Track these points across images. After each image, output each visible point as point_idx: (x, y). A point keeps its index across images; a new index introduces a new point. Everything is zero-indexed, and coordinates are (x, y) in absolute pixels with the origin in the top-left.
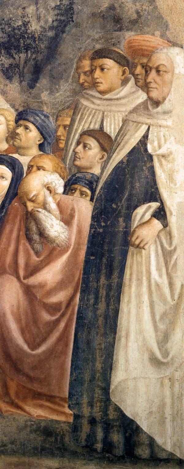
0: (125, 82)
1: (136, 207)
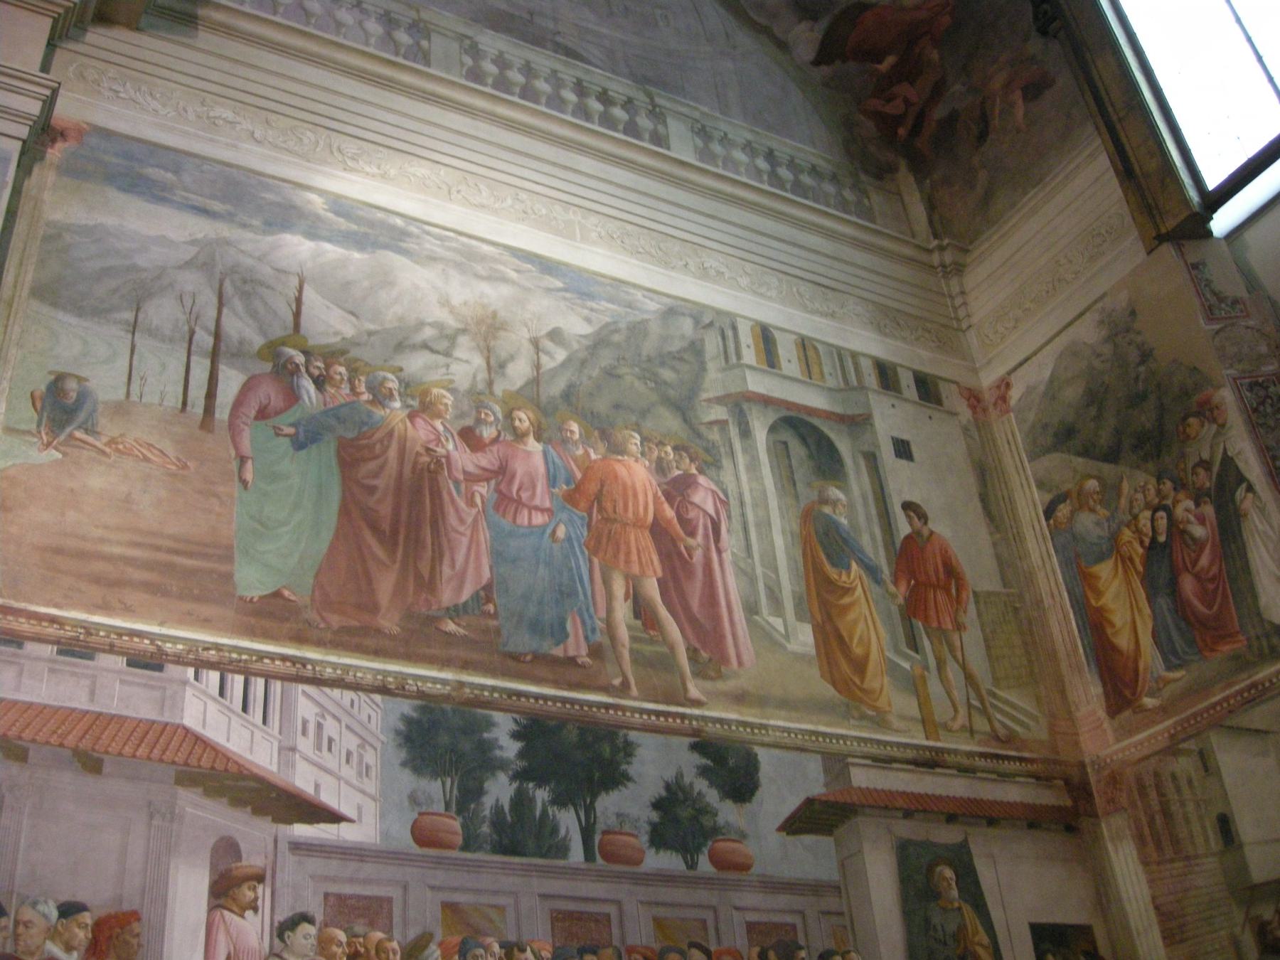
0: (1203, 426)
1: (1235, 491)
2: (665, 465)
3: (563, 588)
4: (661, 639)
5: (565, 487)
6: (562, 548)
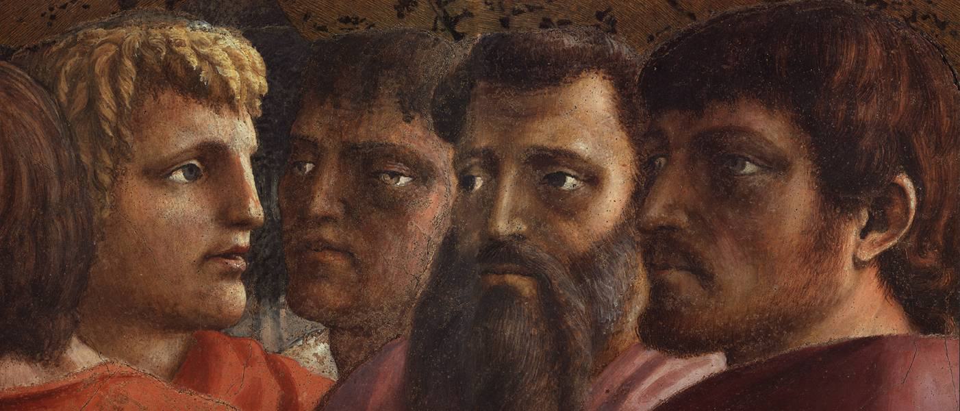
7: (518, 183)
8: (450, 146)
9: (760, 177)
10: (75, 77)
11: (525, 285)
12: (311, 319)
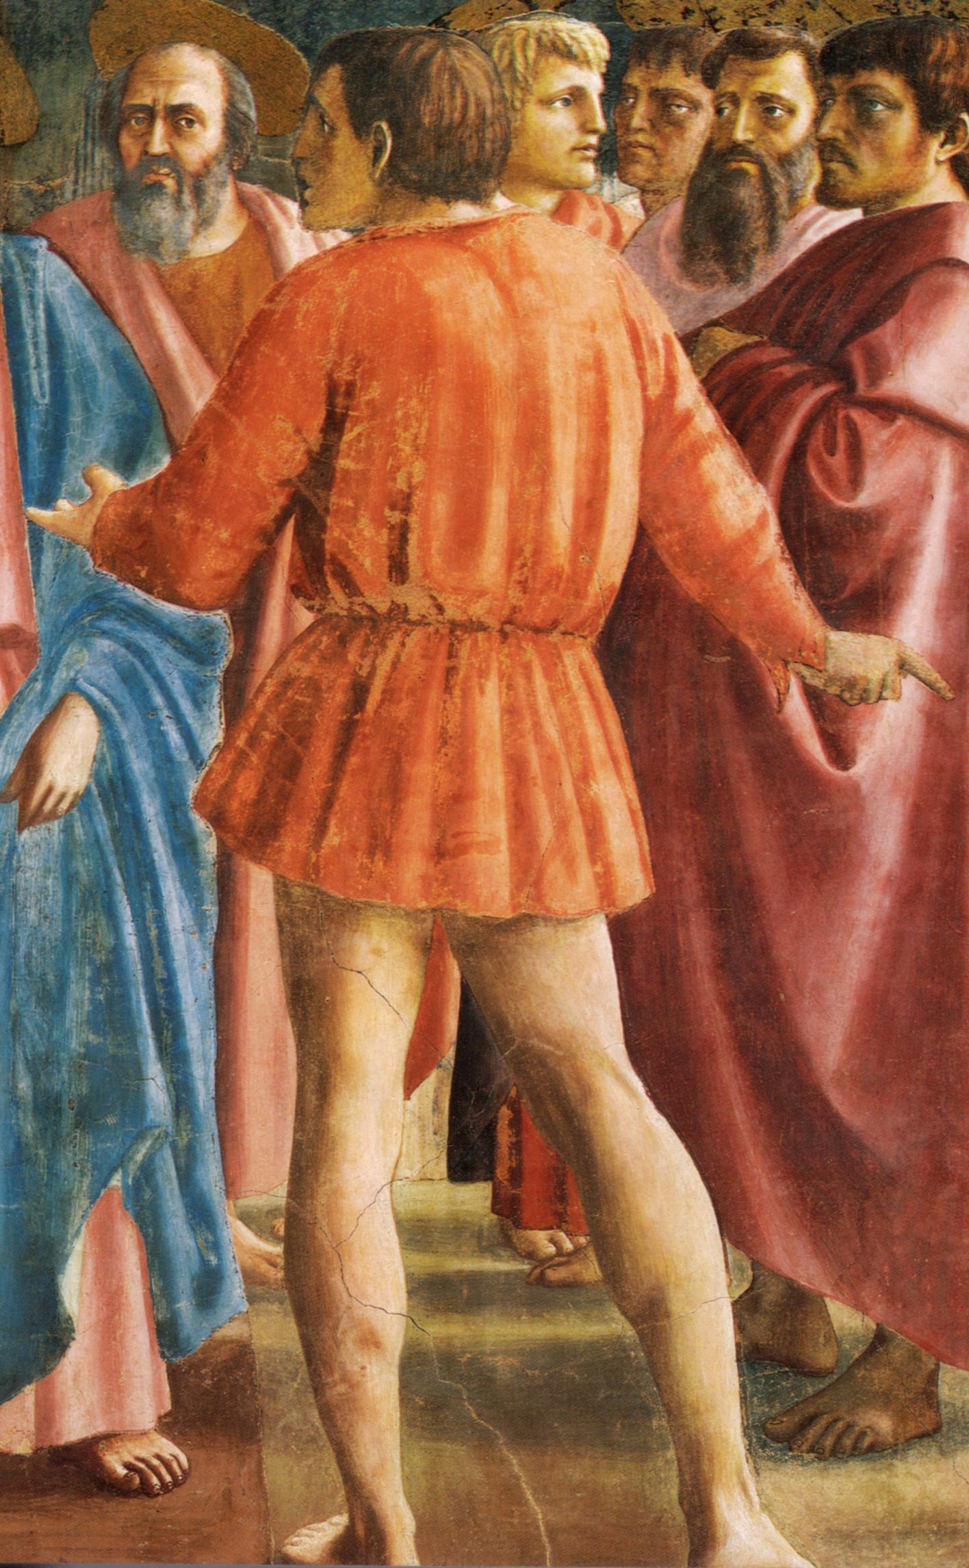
2: (747, 194)
3: (62, 1080)
4: (591, 1270)
5: (112, 481)
6: (68, 853)
7: (749, 111)
8: (708, 90)
9: (886, 112)
10: (503, 47)
11: (751, 168)
12: (631, 185)
